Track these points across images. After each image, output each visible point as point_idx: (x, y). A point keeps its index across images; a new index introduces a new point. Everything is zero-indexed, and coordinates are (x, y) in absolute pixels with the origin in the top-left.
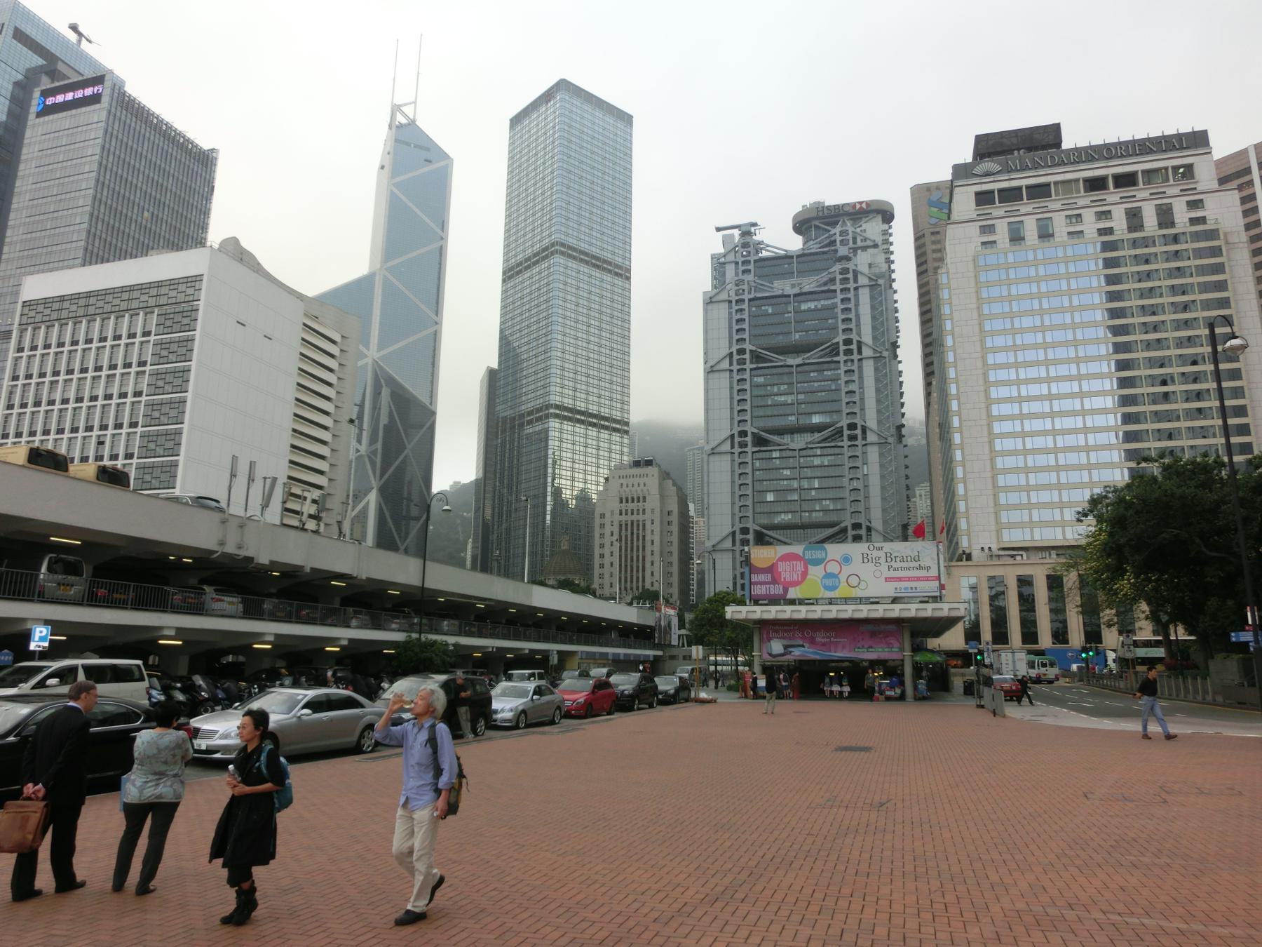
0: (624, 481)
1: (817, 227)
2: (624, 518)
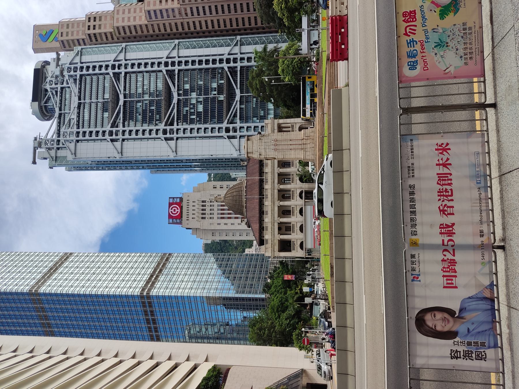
0: (191, 216)
1: (46, 103)
2: (215, 216)
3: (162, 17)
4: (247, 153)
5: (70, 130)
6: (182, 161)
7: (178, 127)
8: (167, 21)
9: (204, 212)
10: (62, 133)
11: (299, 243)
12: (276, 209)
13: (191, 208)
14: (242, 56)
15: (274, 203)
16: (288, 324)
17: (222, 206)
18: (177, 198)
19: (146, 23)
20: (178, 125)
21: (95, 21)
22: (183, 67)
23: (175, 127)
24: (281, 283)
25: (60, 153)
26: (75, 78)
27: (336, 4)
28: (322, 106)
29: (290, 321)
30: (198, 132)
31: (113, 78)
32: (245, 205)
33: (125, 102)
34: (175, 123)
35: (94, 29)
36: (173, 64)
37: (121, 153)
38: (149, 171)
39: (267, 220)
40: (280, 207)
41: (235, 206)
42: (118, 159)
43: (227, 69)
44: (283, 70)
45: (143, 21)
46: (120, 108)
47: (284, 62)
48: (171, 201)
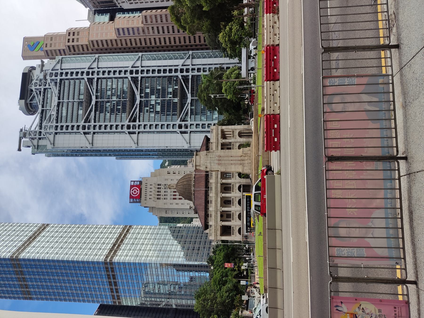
0: (148, 197)
1: (31, 100)
2: (169, 197)
3: (129, 34)
4: (196, 166)
5: (50, 124)
6: (142, 151)
7: (140, 123)
8: (132, 37)
9: (160, 193)
10: (43, 126)
11: (237, 229)
12: (219, 200)
13: (149, 190)
14: (193, 67)
15: (217, 195)
16: (227, 296)
17: (174, 192)
18: (137, 181)
19: (116, 38)
20: (139, 122)
21: (74, 35)
22: (145, 75)
23: (137, 123)
24: (222, 259)
25: (42, 142)
26: (56, 81)
27: (270, 104)
28: (257, 134)
29: (229, 294)
30: (156, 128)
31: (87, 83)
32: (193, 192)
33: (97, 102)
34: (138, 120)
35: (73, 41)
36: (137, 72)
37: (92, 144)
38: (115, 157)
39: (212, 208)
40: (222, 198)
41: (185, 191)
42: (89, 148)
43: (180, 77)
44: (226, 90)
45: (113, 36)
46: (92, 107)
47: (227, 83)
48: (132, 184)
